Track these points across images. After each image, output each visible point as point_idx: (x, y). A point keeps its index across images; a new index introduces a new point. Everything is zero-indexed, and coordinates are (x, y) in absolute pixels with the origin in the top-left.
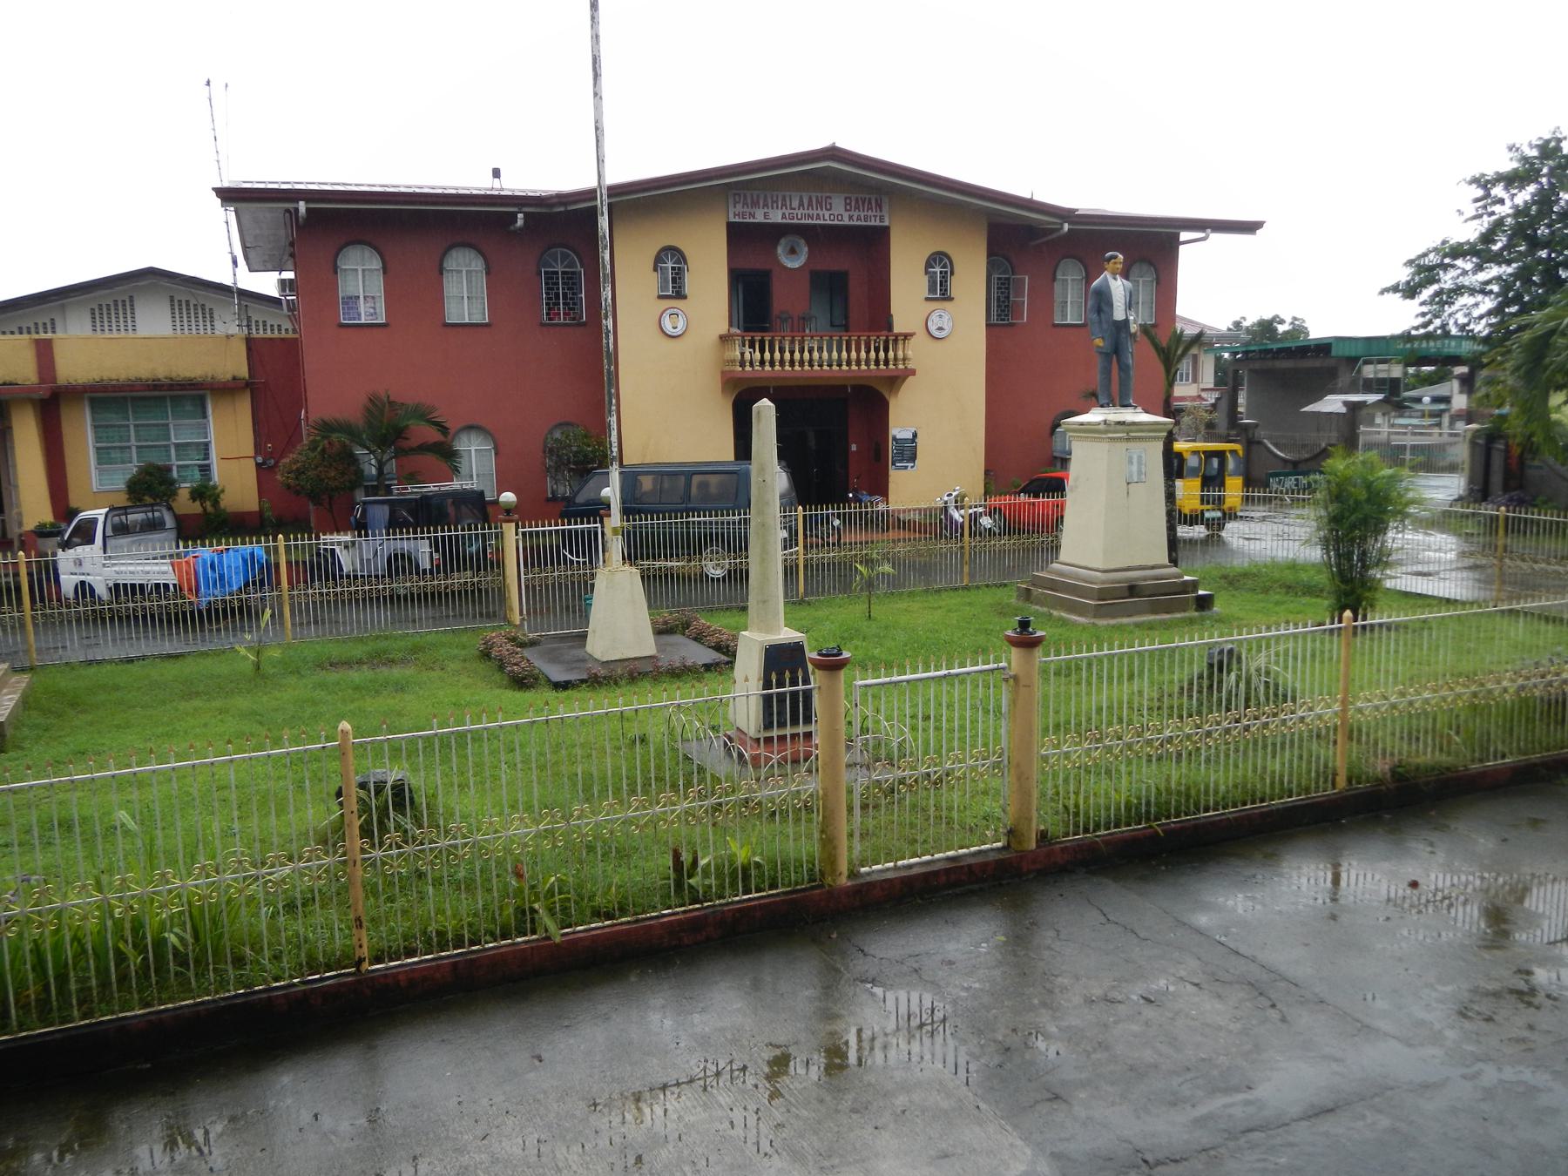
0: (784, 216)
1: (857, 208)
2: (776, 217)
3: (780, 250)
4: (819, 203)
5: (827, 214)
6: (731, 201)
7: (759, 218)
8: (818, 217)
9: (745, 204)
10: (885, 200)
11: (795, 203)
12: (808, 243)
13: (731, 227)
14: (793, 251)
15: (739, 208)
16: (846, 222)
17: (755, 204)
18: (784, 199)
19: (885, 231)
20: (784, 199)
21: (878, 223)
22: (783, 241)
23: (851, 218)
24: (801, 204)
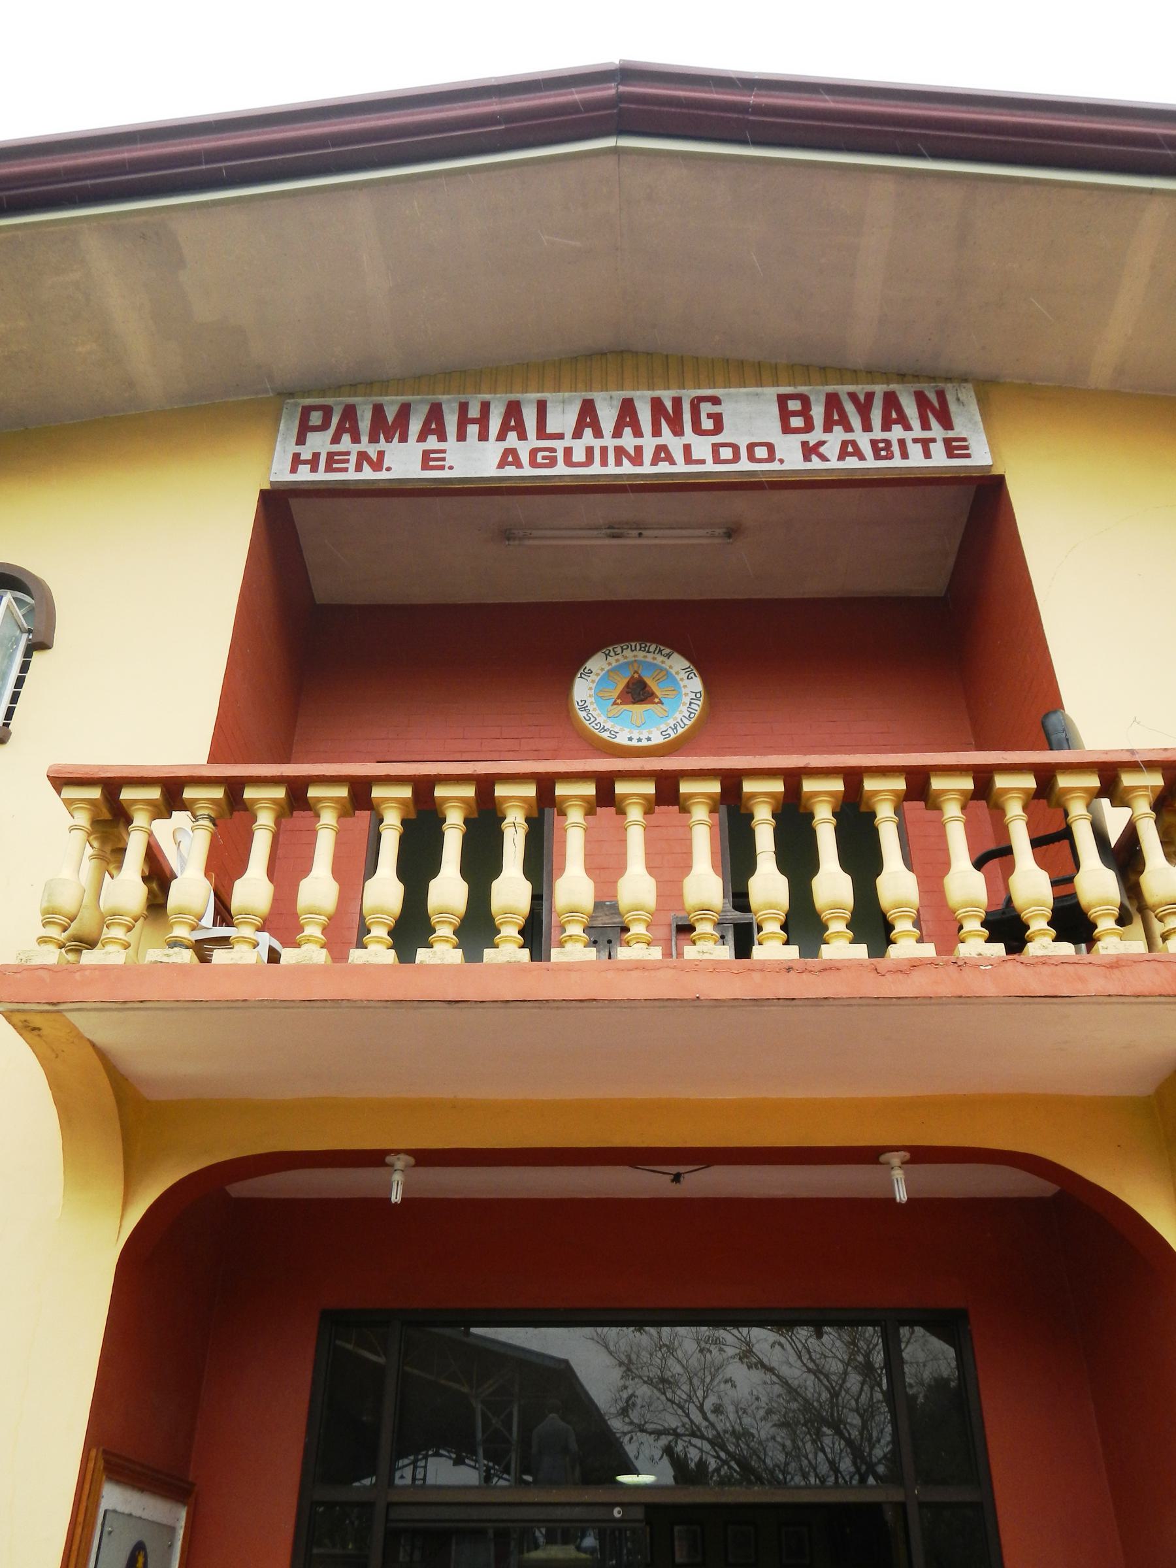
0: (509, 457)
1: (835, 415)
2: (474, 459)
3: (582, 690)
4: (668, 416)
5: (702, 447)
6: (288, 427)
7: (403, 461)
8: (662, 454)
9: (349, 424)
10: (968, 394)
11: (563, 418)
12: (702, 664)
13: (279, 514)
14: (638, 692)
15: (319, 442)
16: (790, 457)
17: (389, 427)
18: (513, 411)
19: (983, 503)
20: (513, 411)
21: (939, 459)
22: (597, 664)
23: (809, 451)
24: (587, 417)
